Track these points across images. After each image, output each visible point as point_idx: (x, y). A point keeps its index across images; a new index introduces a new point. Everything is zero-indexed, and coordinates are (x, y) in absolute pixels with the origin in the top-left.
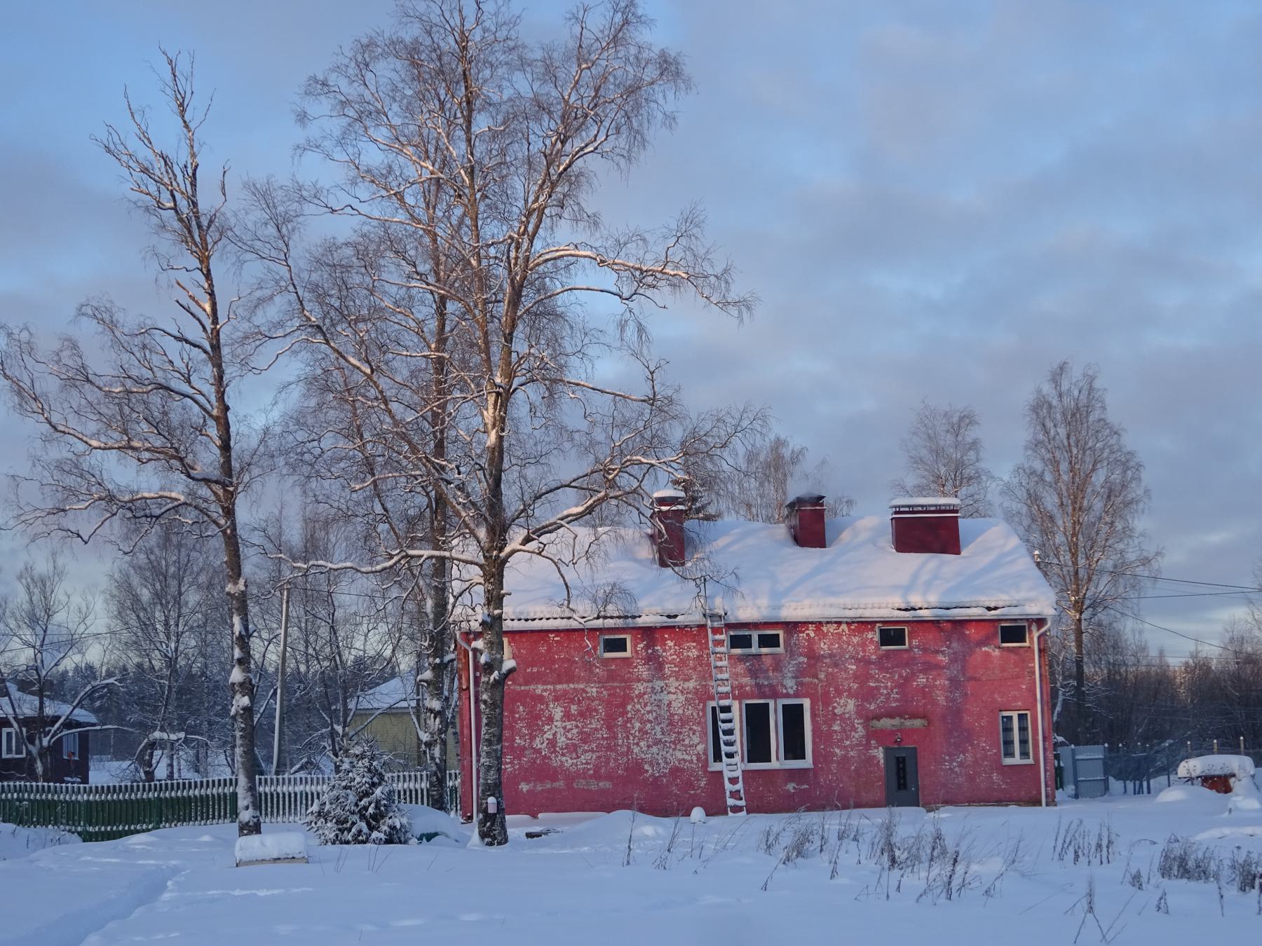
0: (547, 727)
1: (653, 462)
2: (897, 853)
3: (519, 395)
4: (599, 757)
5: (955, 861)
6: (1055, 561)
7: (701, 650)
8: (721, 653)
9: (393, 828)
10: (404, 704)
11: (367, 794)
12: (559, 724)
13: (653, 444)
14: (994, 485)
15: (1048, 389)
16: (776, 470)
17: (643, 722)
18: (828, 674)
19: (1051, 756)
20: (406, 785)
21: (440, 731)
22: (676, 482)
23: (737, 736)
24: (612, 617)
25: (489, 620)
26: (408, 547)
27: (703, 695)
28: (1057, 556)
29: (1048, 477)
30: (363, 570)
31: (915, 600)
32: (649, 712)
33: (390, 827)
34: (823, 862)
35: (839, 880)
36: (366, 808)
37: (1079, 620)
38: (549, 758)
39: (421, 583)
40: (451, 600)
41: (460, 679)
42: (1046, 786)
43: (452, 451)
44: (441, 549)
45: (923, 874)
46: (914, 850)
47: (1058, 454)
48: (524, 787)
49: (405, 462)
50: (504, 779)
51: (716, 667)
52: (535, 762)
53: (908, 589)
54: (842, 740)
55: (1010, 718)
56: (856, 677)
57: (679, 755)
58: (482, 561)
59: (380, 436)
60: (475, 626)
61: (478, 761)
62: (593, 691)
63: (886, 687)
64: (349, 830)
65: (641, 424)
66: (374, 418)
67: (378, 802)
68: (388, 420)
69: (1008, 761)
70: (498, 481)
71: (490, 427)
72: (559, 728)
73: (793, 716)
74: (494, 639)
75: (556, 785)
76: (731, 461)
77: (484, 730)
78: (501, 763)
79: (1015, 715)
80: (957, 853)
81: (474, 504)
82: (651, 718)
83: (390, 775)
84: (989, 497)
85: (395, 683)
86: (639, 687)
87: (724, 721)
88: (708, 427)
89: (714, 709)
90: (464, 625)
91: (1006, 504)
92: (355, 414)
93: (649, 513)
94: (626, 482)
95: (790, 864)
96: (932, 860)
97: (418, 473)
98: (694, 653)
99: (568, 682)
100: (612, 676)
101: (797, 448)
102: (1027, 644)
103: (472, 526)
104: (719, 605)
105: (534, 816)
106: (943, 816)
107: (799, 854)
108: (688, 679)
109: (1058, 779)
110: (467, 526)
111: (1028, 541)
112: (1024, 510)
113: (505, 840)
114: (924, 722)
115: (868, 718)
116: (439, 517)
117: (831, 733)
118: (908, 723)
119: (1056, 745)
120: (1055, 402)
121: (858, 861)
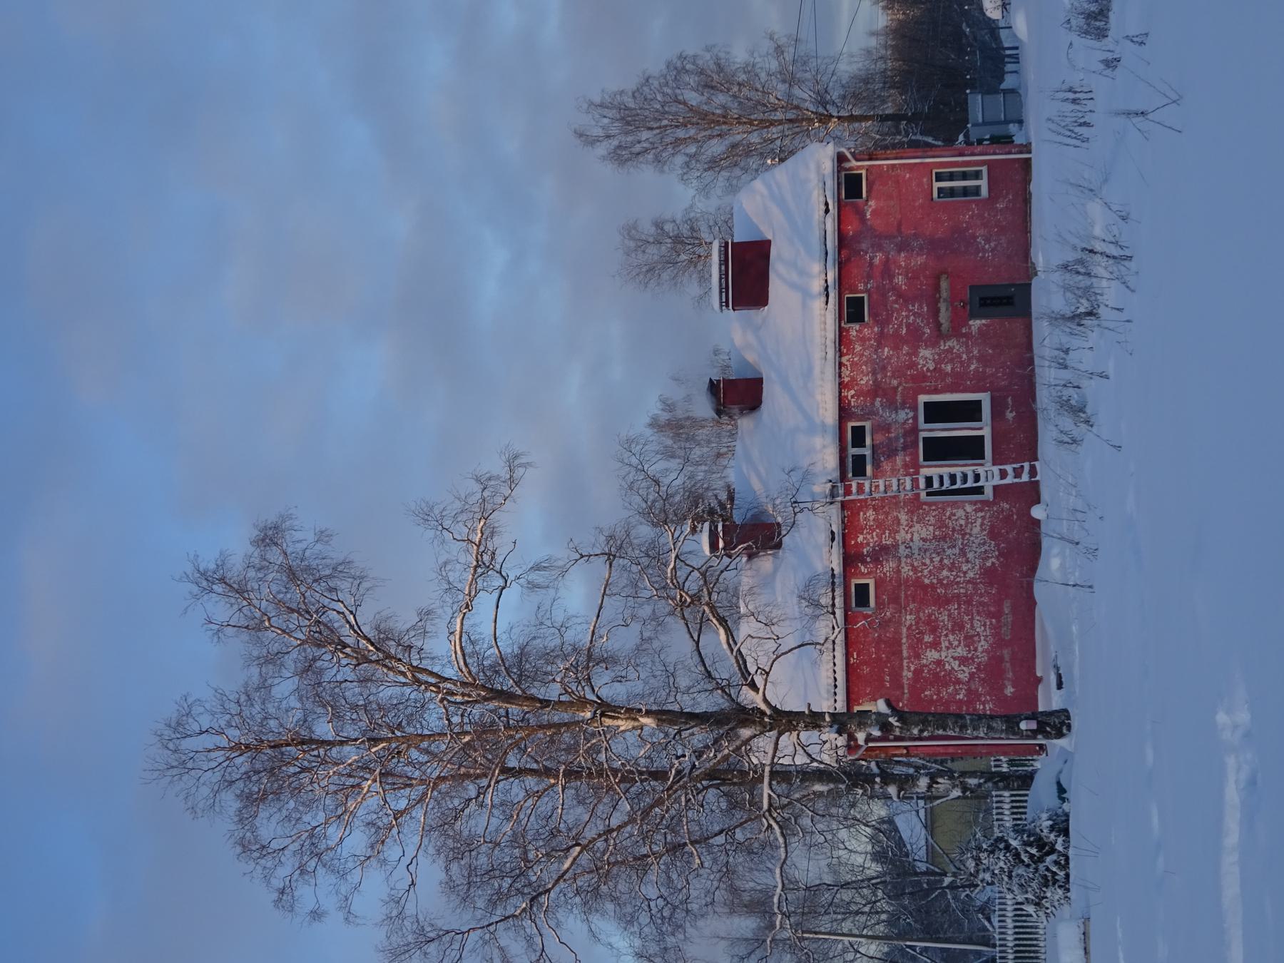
0: (947, 667)
1: (673, 556)
2: (1082, 310)
3: (605, 693)
4: (979, 613)
5: (1091, 251)
6: (778, 142)
7: (867, 507)
8: (873, 486)
9: (1052, 828)
10: (922, 813)
11: (1017, 855)
12: (944, 654)
13: (655, 555)
14: (699, 205)
15: (602, 149)
16: (682, 427)
17: (942, 567)
18: (893, 376)
19: (979, 149)
20: (1007, 812)
21: (951, 778)
22: (694, 530)
23: (957, 471)
24: (833, 598)
25: (836, 727)
26: (760, 808)
27: (915, 505)
28: (773, 141)
29: (692, 149)
30: (783, 856)
31: (817, 286)
32: (932, 561)
33: (1051, 831)
34: (1090, 386)
35: (1111, 372)
36: (1032, 856)
37: (839, 118)
38: (979, 664)
39: (797, 796)
40: (815, 764)
41: (896, 755)
42: (1010, 153)
43: (661, 762)
44: (762, 776)
45: (1104, 283)
46: (1079, 293)
47: (668, 140)
48: (1009, 690)
49: (673, 812)
50: (1001, 711)
51: (885, 492)
53: (806, 294)
54: (962, 363)
55: (939, 189)
56: (896, 348)
57: (976, 530)
58: (774, 733)
59: (645, 837)
60: (841, 741)
61: (982, 738)
62: (909, 619)
63: (907, 317)
64: (1054, 874)
65: (635, 568)
66: (627, 843)
67: (1025, 844)
68: (629, 828)
69: (984, 192)
70: (692, 716)
71: (636, 724)
72: (948, 654)
73: (936, 412)
74: (856, 721)
75: (1007, 657)
76: (673, 476)
77: (950, 733)
78: (985, 715)
79: (936, 185)
80: (1084, 249)
81: (716, 741)
82: (938, 559)
83: (996, 829)
84: (712, 210)
85: (900, 822)
86: (906, 571)
87: (942, 484)
88: (638, 499)
89: (928, 494)
90: (840, 752)
91: (719, 192)
92: (623, 862)
93: (726, 560)
94: (693, 584)
95: (1092, 420)
96: (1089, 274)
97: (683, 799)
98: (871, 514)
99: (900, 645)
100: (895, 599)
101: (660, 405)
102: (864, 172)
103: (738, 743)
104: (821, 488)
105: (1039, 680)
106: (1041, 259)
107: (1082, 410)
108: (898, 521)
109: (1003, 141)
110: (739, 748)
111: (757, 170)
112: (725, 174)
113: (1065, 713)
114: (944, 277)
115: (939, 335)
116: (731, 777)
117: (954, 374)
118: (944, 294)
119: (968, 142)
120: (615, 143)
121: (1090, 349)
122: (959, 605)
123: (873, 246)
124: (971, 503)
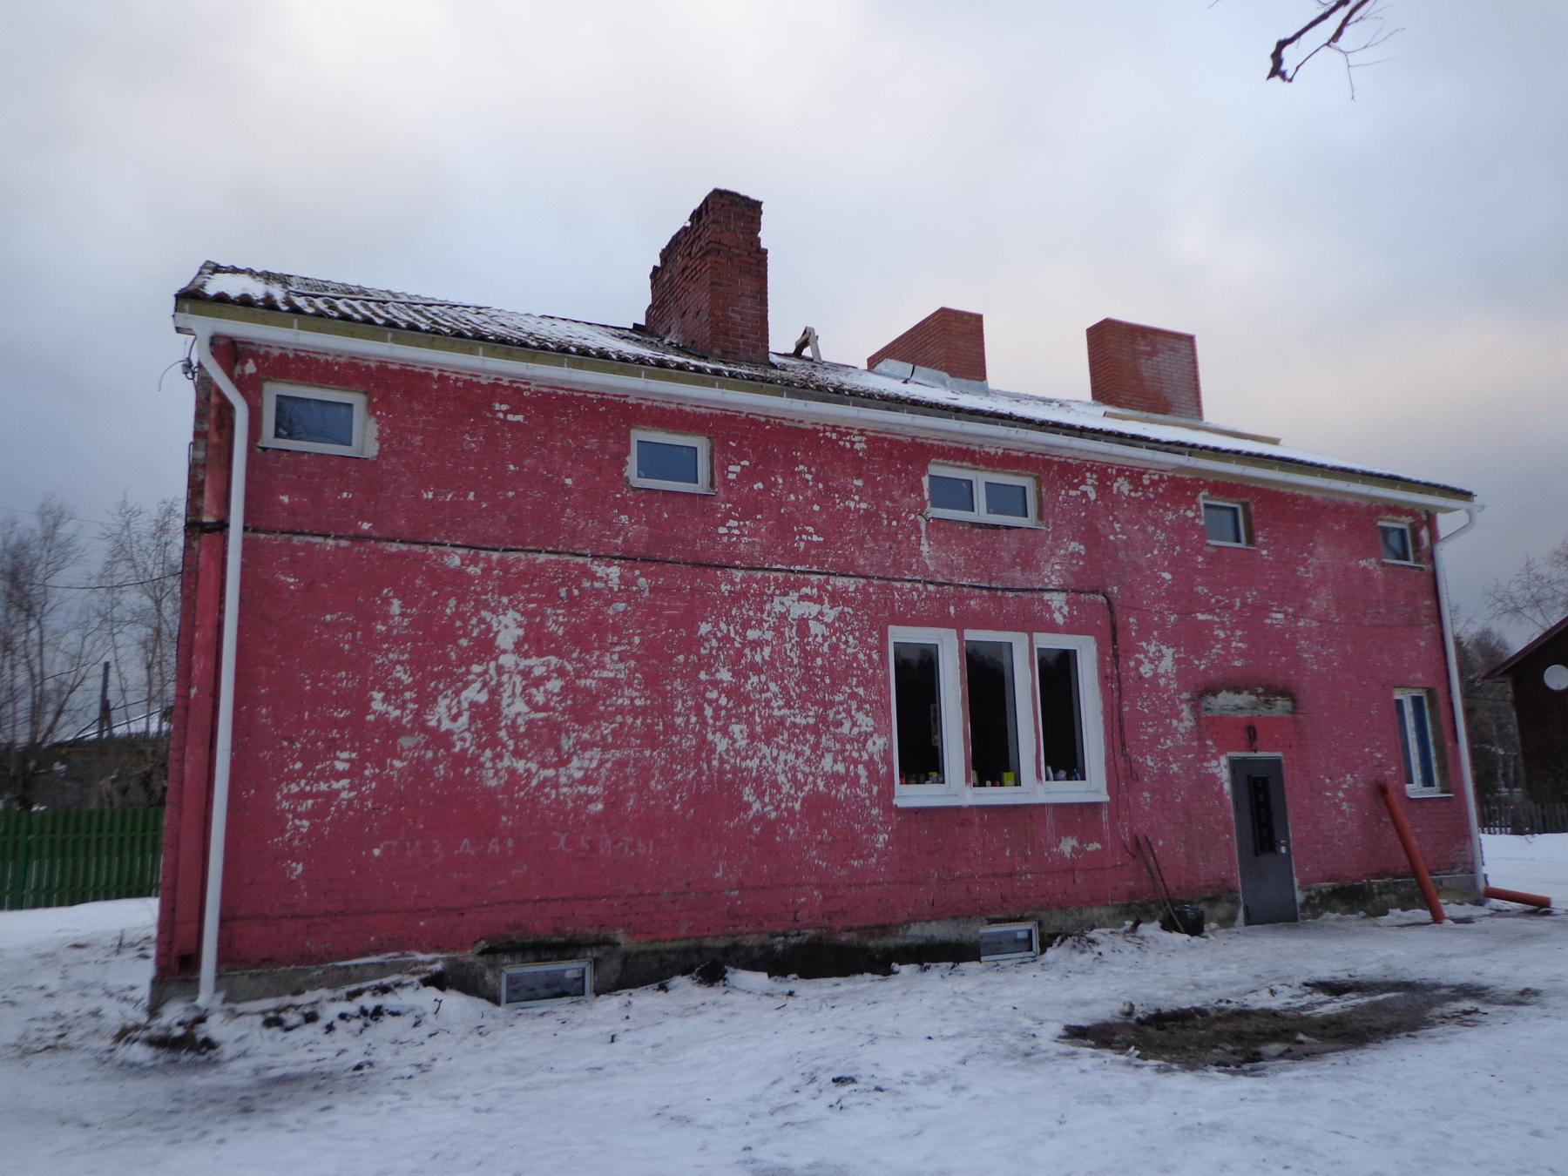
4: (621, 764)
12: (508, 660)
52: (430, 774)
54: (1156, 738)
63: (1223, 626)
73: (1057, 675)
114: (1288, 704)
122: (643, 711)
123: (1322, 567)
124: (887, 753)
